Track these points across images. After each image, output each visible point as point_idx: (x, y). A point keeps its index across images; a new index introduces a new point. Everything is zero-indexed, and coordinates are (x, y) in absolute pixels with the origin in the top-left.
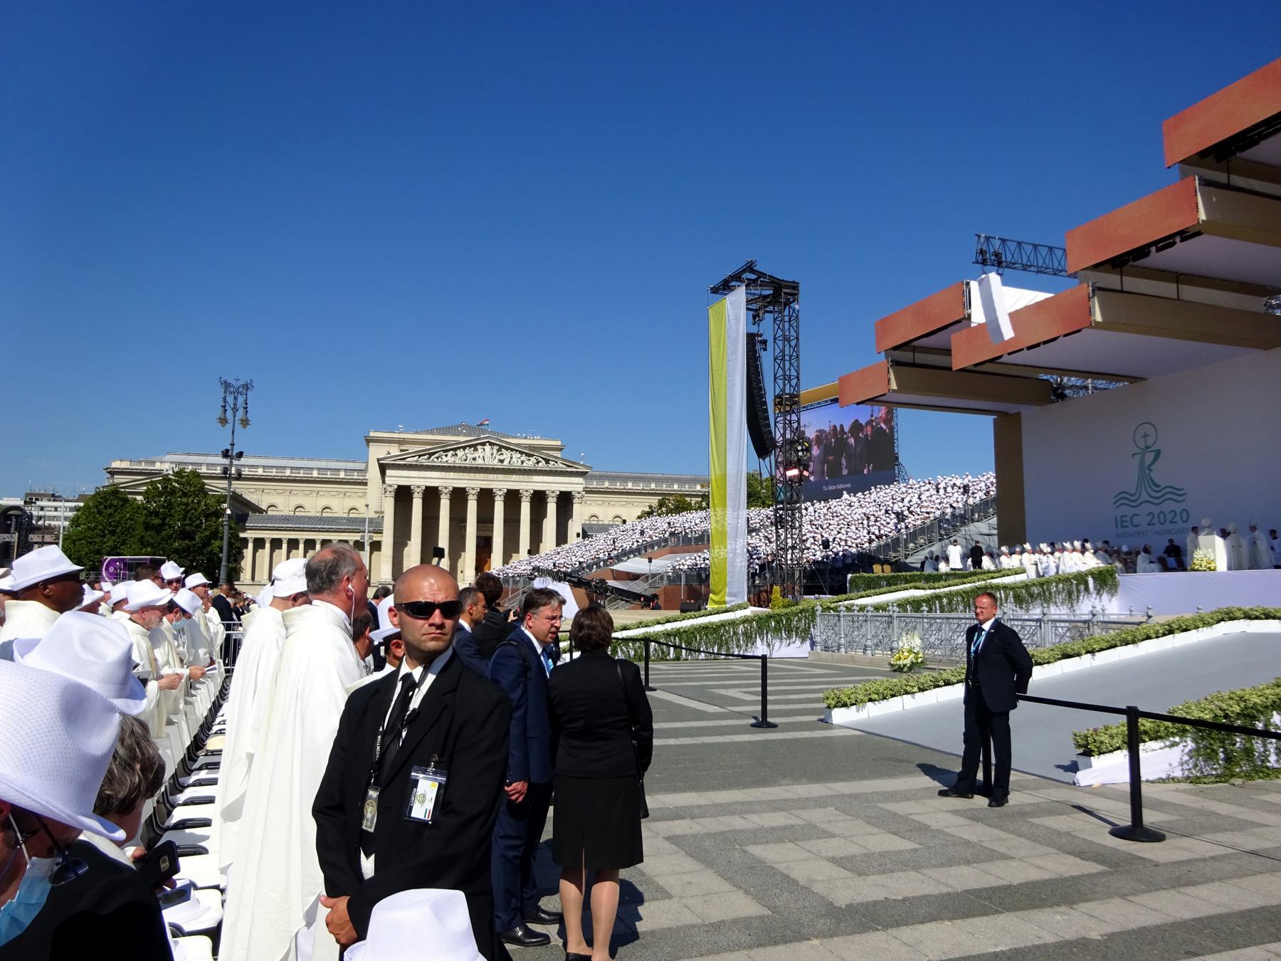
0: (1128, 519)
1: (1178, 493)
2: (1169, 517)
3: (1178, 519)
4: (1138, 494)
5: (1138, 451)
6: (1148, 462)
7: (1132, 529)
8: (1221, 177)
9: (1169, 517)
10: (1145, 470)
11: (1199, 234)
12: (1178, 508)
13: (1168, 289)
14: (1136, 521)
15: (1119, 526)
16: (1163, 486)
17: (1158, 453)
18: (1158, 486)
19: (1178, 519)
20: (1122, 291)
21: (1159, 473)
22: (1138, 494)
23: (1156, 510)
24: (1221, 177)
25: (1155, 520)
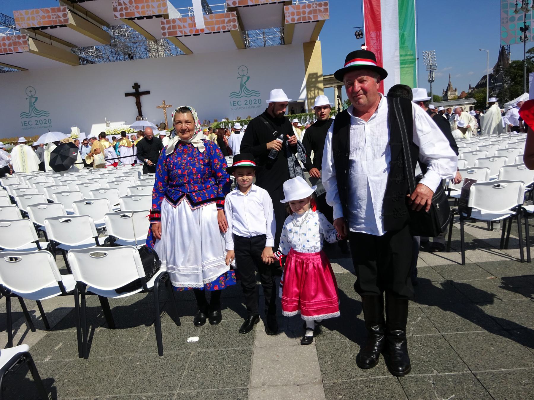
0: (27, 122)
1: (46, 113)
2: (44, 122)
3: (47, 122)
4: (30, 113)
5: (28, 97)
6: (33, 101)
7: (29, 126)
8: (72, 9)
9: (44, 122)
10: (32, 106)
11: (65, 26)
12: (47, 118)
13: (47, 40)
14: (30, 123)
15: (23, 125)
16: (40, 110)
17: (37, 98)
18: (38, 111)
19: (47, 122)
20: (36, 39)
21: (37, 105)
22: (30, 113)
23: (38, 119)
24: (72, 9)
25: (38, 123)
